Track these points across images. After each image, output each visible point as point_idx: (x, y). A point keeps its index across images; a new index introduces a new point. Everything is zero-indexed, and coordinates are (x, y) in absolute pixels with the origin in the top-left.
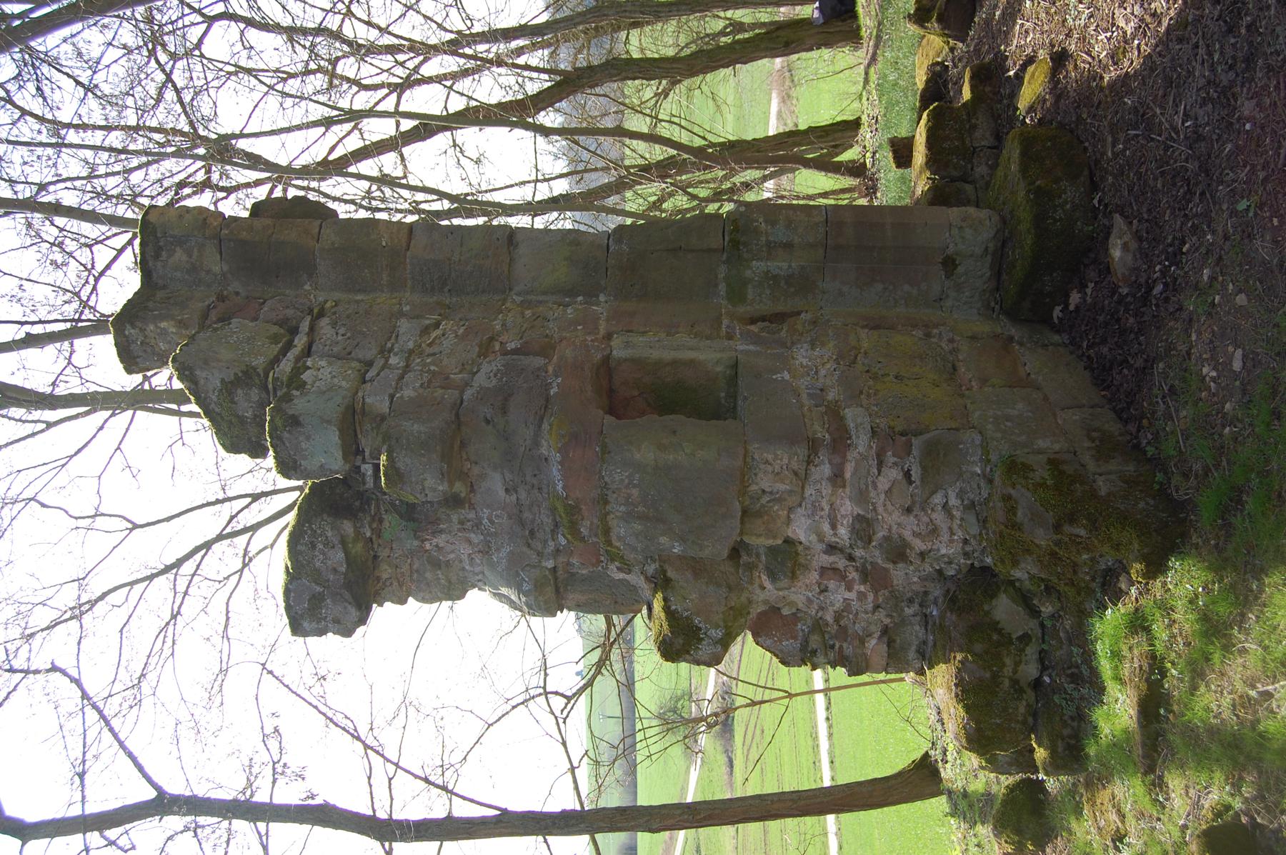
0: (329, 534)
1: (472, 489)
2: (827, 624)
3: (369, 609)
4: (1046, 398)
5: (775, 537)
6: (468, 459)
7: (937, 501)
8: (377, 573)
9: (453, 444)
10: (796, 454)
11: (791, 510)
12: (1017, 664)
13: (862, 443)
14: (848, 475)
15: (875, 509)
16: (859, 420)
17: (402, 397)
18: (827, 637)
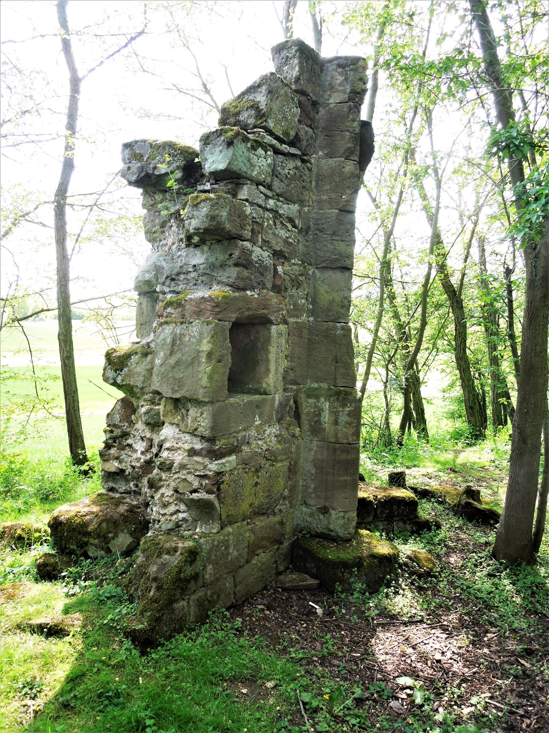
0: (174, 165)
1: (196, 246)
2: (126, 439)
3: (138, 186)
4: (241, 567)
5: (164, 416)
6: (212, 244)
7: (181, 506)
8: (158, 192)
9: (211, 236)
10: (206, 430)
11: (178, 425)
12: (95, 546)
13: (214, 466)
14: (196, 458)
15: (176, 473)
16: (227, 464)
17: (246, 206)
18: (120, 439)
